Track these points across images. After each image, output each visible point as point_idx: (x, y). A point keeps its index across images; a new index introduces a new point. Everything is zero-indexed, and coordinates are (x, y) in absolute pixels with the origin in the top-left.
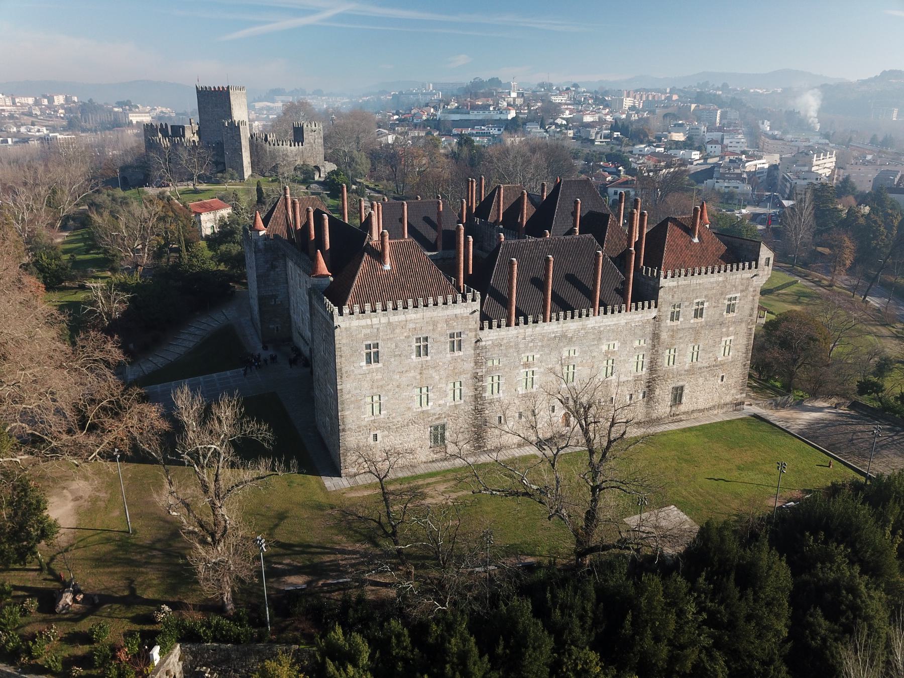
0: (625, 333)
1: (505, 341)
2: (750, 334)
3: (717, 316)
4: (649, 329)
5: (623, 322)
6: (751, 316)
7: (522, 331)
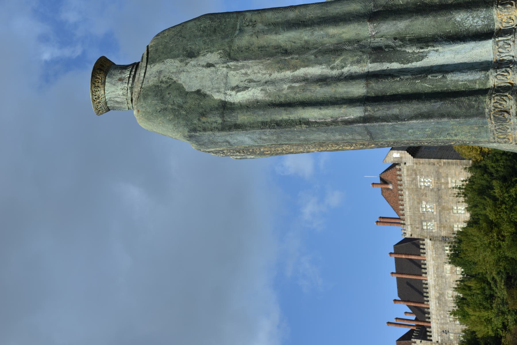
0: (439, 261)
2: (448, 163)
3: (433, 193)
4: (438, 244)
5: (432, 262)
6: (434, 164)
7: (434, 321)
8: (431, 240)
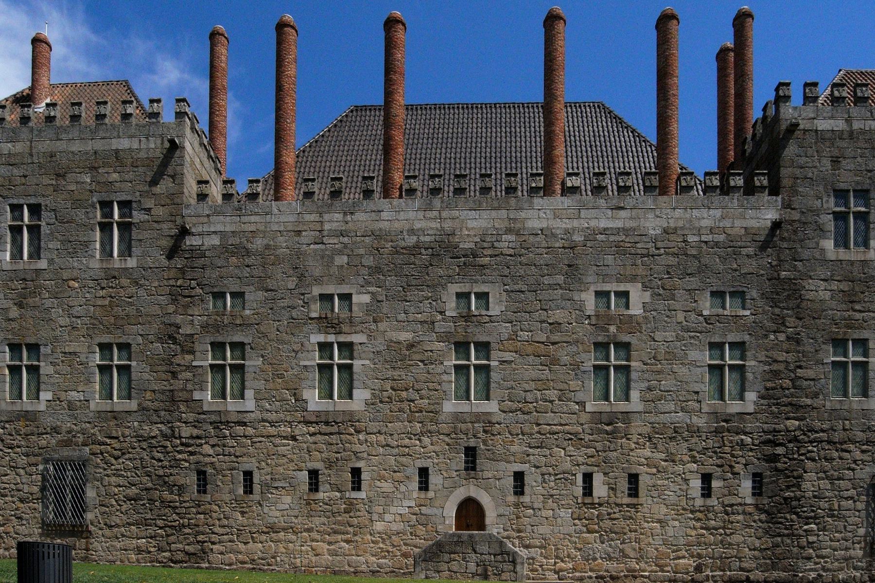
1: (259, 243)
5: (652, 225)
8: (776, 225)
